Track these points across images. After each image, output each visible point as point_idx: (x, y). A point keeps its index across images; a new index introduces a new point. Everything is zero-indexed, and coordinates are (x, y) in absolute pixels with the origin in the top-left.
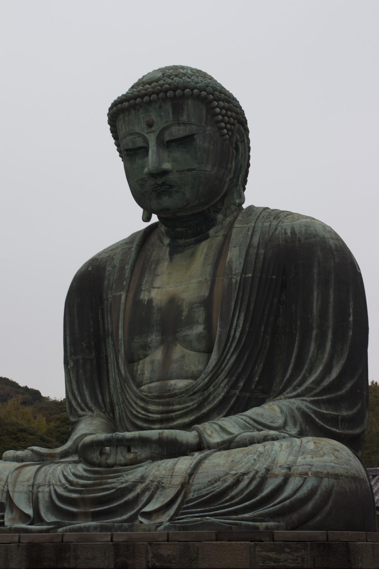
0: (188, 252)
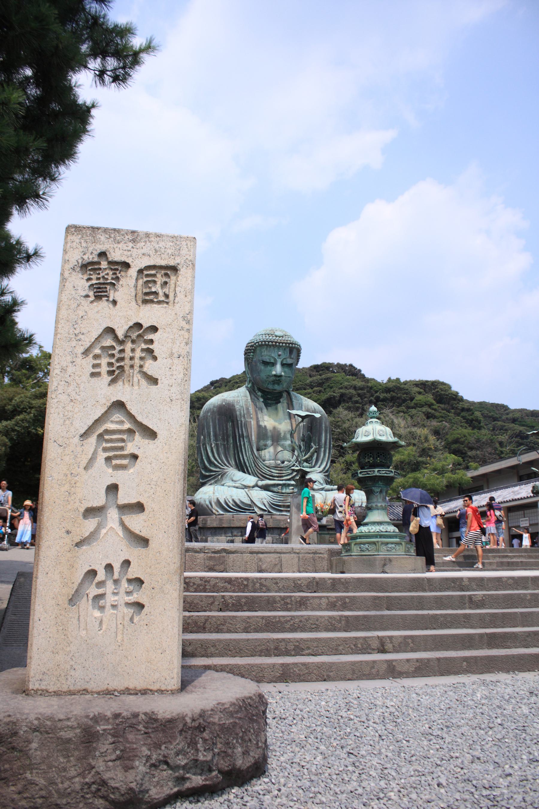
0: (274, 407)
